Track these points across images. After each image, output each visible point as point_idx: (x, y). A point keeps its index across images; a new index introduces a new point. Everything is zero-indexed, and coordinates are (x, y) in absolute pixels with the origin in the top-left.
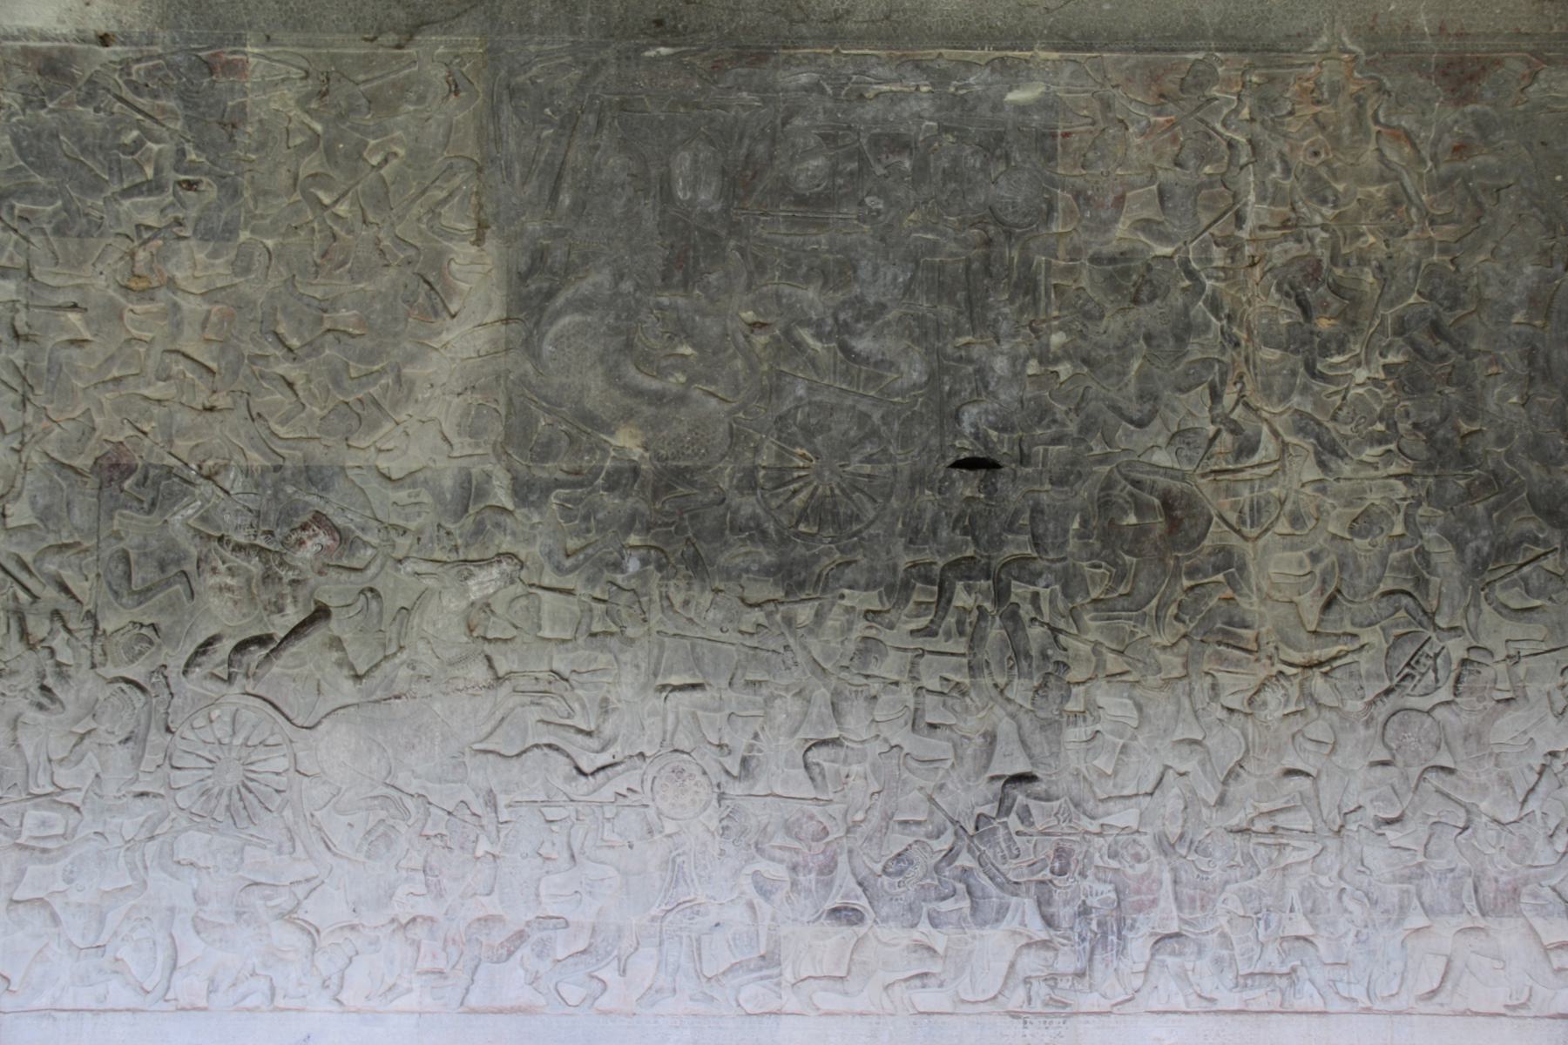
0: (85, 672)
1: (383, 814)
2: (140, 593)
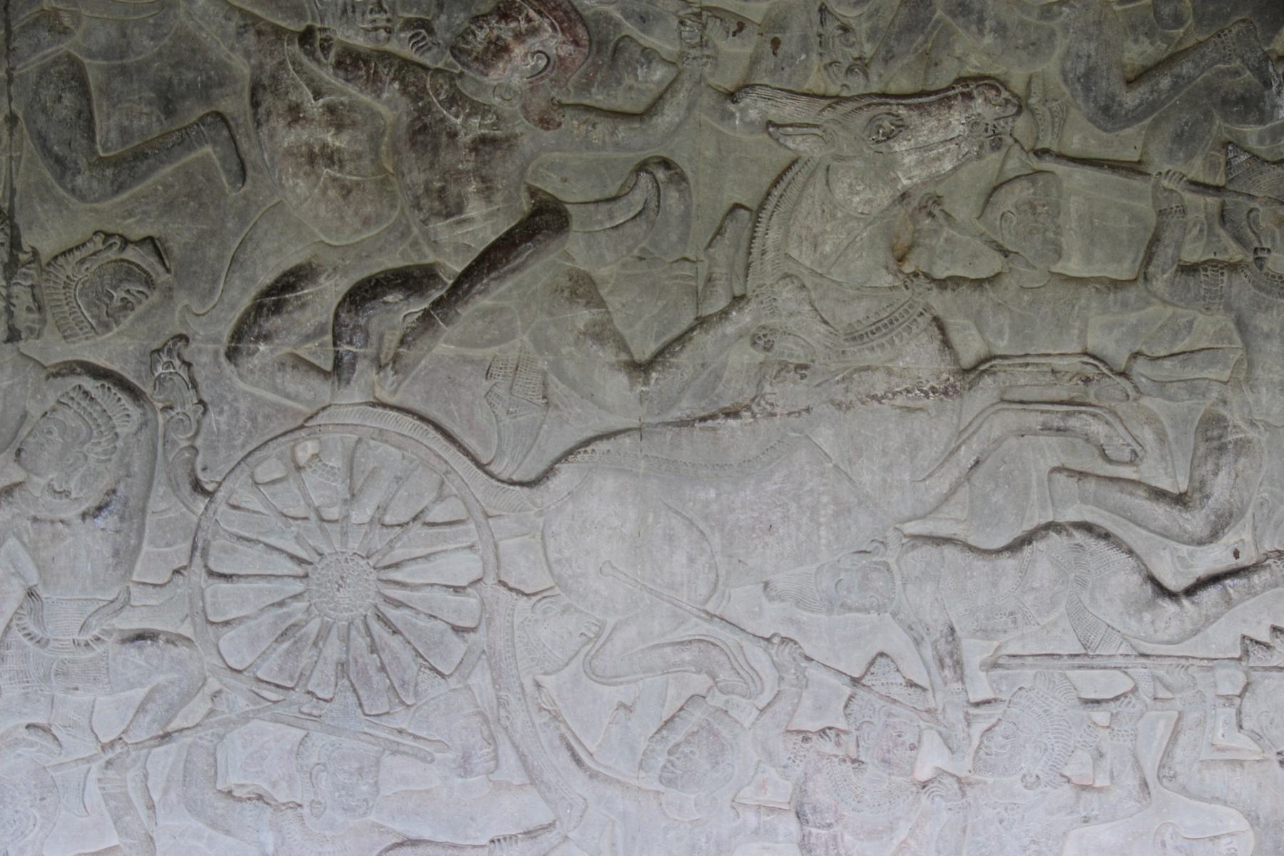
1: (700, 683)
2: (116, 162)
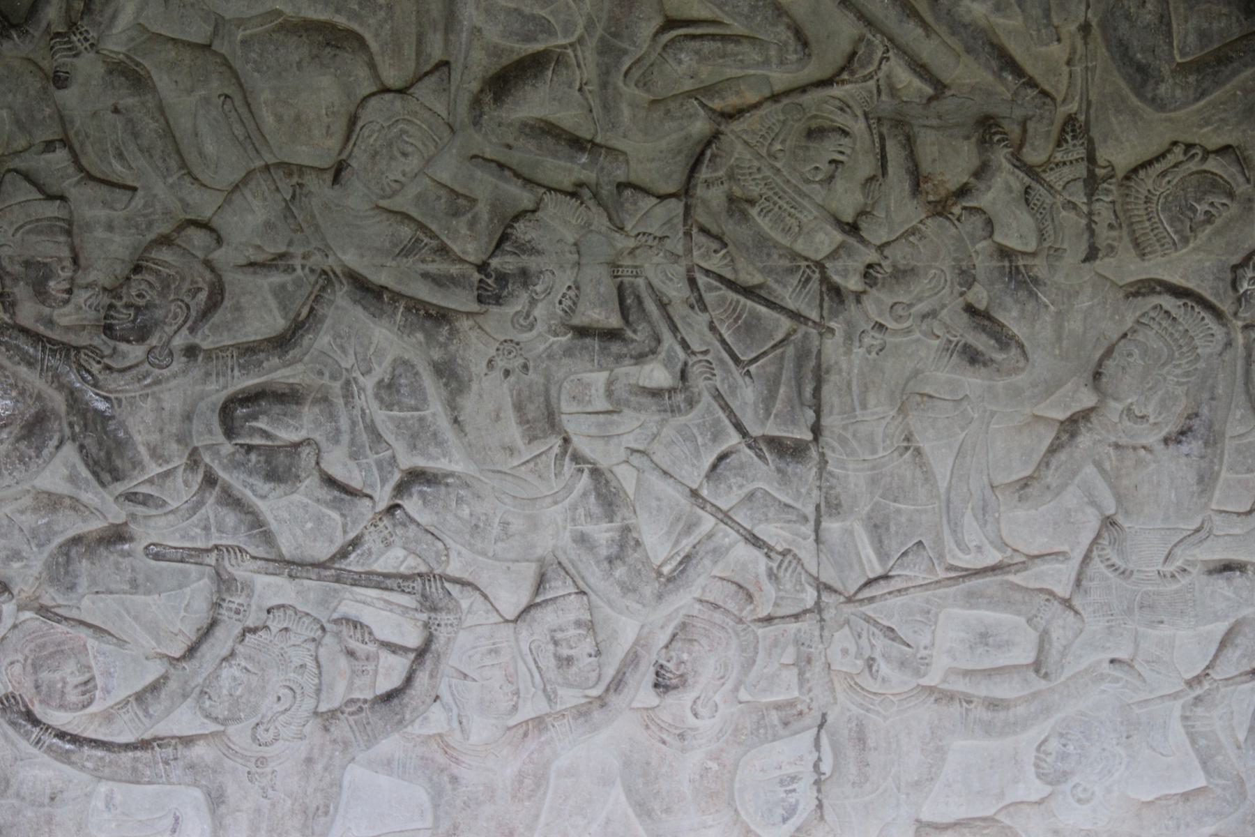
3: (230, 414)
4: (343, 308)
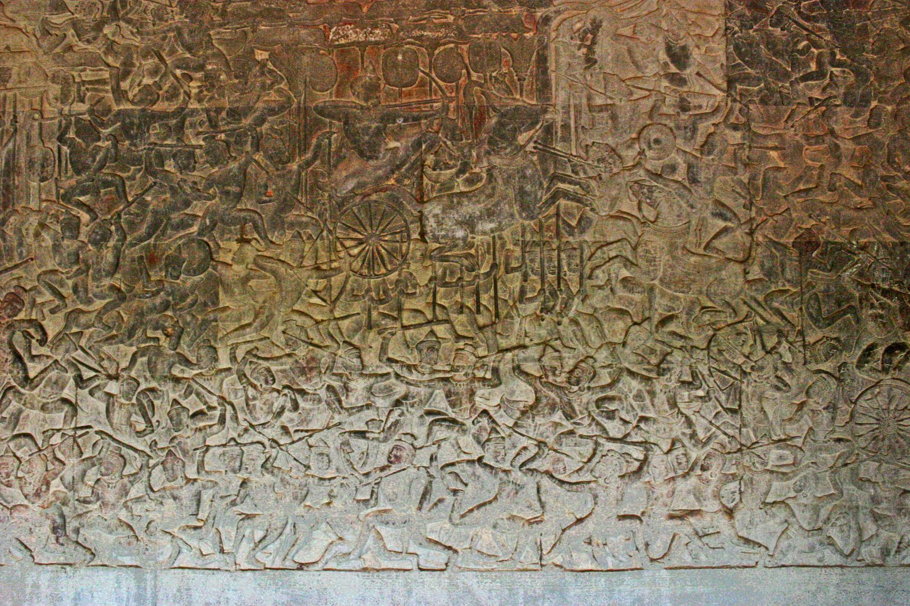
0: (799, 369)
3: (599, 402)
4: (626, 378)
